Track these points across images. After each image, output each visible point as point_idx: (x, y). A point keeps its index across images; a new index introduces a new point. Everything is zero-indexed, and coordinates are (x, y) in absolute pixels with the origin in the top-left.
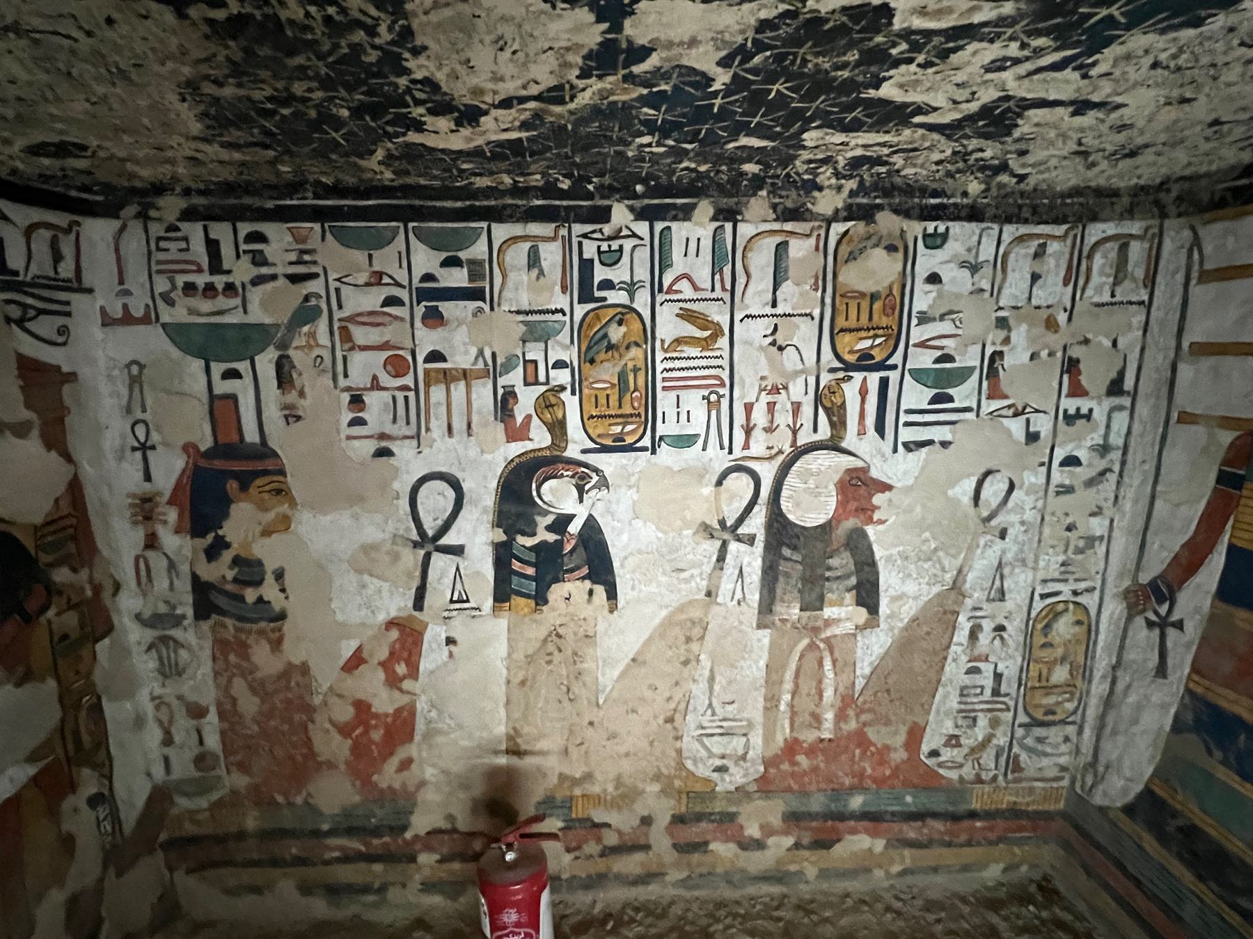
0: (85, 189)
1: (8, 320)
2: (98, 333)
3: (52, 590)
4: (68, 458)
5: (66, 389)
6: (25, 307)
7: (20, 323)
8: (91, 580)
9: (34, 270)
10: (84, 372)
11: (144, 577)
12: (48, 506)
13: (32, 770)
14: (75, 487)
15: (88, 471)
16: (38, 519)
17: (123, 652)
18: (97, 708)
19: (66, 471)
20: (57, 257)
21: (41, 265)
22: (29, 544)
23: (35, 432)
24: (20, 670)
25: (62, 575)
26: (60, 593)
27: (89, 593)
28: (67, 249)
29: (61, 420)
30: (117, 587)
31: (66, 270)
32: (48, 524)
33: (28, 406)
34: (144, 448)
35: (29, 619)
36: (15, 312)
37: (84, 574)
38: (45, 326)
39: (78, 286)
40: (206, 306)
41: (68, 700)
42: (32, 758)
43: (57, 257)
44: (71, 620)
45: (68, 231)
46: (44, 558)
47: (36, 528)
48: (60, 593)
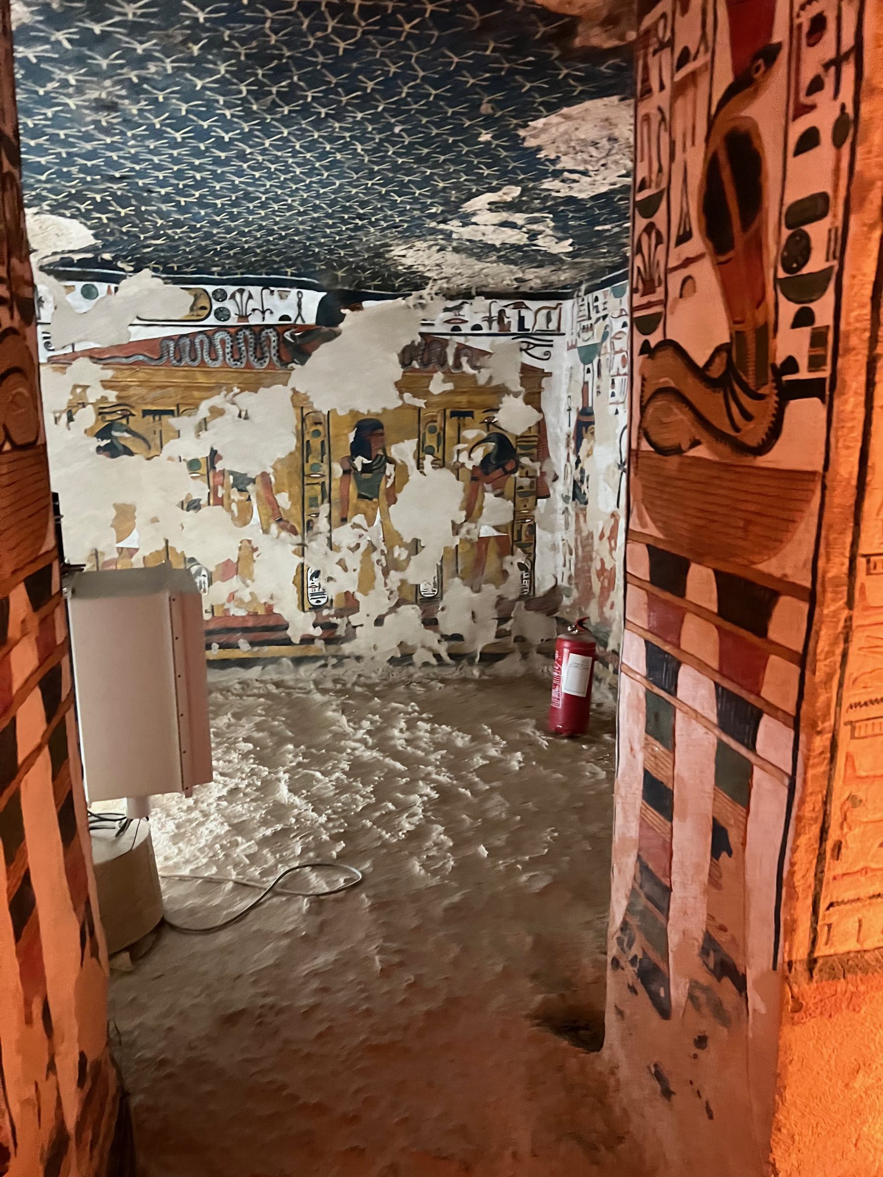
0: (564, 287)
1: (521, 350)
2: (566, 354)
3: (518, 466)
4: (540, 410)
5: (544, 379)
6: (529, 343)
7: (525, 350)
8: (541, 468)
9: (536, 328)
10: (556, 373)
11: (565, 478)
12: (525, 429)
13: (496, 534)
14: (541, 426)
15: (550, 419)
16: (519, 434)
17: (551, 510)
18: (532, 529)
19: (535, 416)
20: (549, 320)
21: (541, 324)
22: (513, 442)
23: (521, 397)
24: (498, 491)
25: (525, 460)
26: (523, 468)
27: (539, 474)
28: (554, 316)
29: (539, 393)
30: (556, 478)
31: (553, 326)
32: (522, 437)
33: (522, 385)
34: (569, 410)
35: (507, 473)
36: (525, 346)
37: (537, 465)
38: (538, 352)
39: (558, 332)
40: (585, 336)
41: (518, 517)
42: (497, 528)
43: (549, 320)
44: (526, 482)
45: (555, 308)
46: (519, 451)
47: (517, 437)
48: (523, 468)
